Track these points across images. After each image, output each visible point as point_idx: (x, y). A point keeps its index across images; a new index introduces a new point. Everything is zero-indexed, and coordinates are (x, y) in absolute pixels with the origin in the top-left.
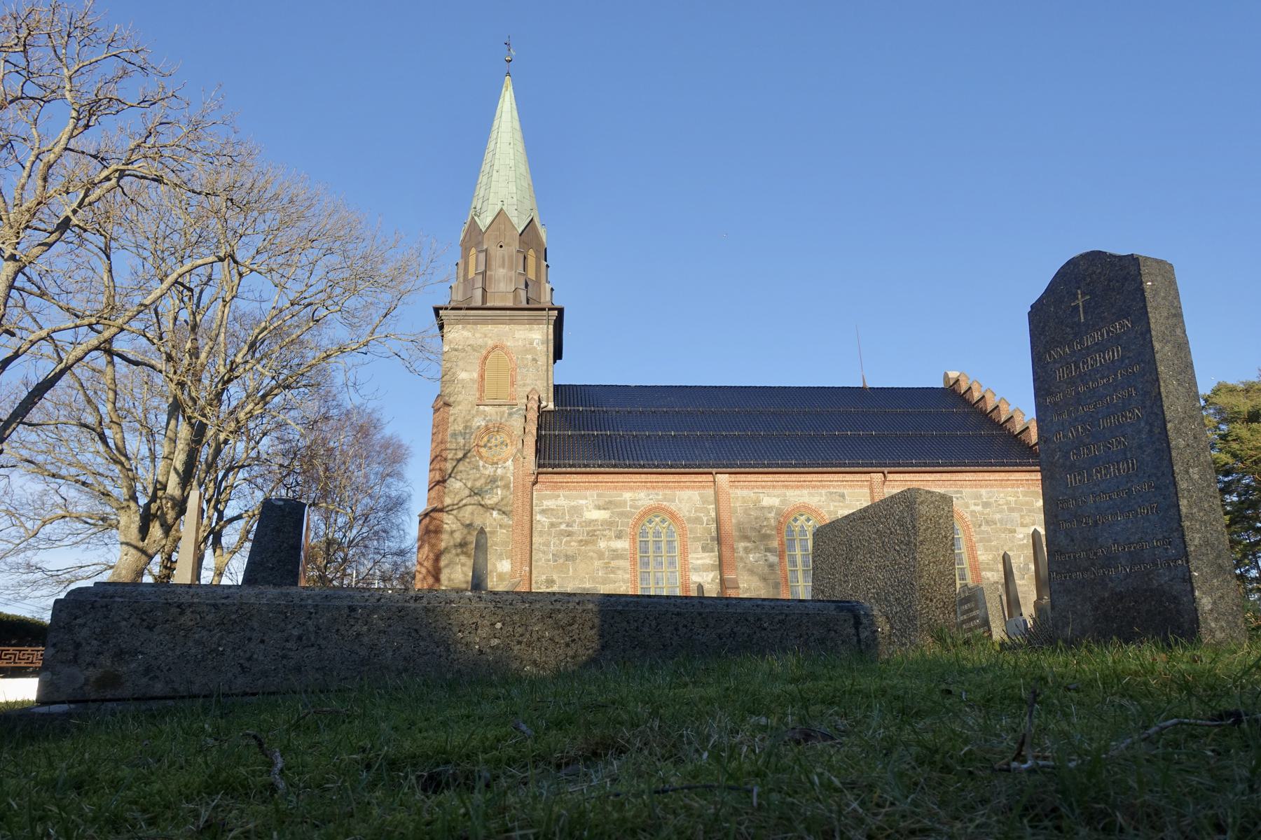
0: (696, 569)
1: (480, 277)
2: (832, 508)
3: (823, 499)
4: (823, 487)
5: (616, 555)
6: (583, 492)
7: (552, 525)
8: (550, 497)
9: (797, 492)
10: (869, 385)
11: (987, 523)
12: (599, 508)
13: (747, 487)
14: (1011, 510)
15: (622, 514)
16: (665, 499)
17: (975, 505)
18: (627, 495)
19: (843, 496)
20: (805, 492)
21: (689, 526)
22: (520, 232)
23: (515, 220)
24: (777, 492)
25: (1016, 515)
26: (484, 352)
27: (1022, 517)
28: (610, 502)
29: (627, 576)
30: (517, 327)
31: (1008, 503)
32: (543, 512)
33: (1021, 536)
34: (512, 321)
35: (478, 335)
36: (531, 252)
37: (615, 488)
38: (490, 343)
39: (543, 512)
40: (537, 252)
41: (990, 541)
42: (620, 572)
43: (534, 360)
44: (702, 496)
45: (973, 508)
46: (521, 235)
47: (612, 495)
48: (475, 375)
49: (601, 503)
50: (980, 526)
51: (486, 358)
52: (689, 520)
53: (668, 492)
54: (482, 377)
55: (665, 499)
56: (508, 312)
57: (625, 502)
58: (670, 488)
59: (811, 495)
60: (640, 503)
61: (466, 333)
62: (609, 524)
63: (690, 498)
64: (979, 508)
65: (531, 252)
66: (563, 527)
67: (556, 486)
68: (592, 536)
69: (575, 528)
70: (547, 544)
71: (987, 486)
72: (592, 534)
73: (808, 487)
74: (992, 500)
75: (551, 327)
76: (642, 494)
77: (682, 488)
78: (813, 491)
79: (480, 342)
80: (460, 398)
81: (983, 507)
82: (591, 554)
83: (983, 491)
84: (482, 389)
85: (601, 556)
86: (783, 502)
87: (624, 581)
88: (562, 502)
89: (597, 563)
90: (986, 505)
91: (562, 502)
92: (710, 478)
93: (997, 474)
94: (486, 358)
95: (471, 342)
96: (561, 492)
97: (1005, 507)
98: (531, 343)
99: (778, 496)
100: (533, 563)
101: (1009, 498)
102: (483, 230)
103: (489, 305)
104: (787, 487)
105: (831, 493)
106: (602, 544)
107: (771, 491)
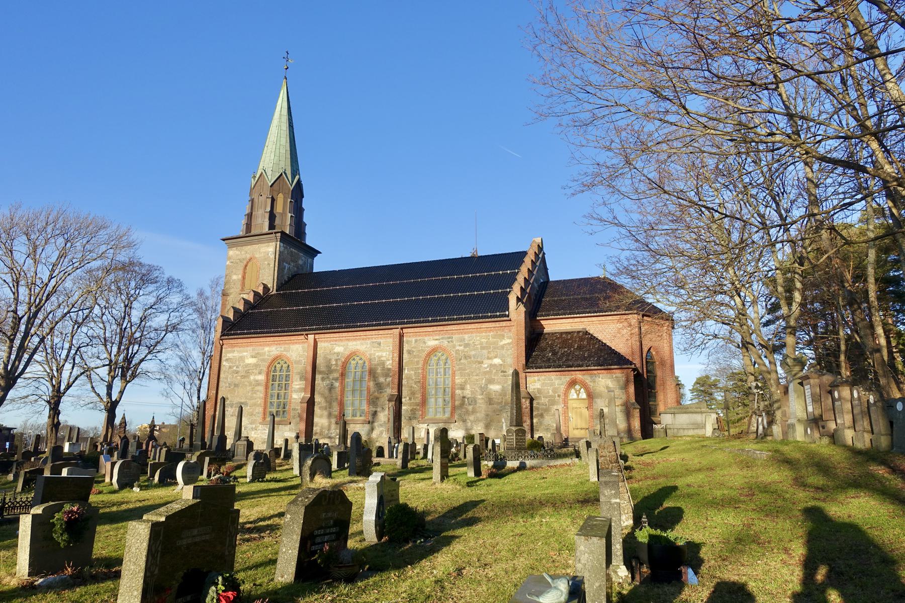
2: (373, 352)
3: (368, 346)
4: (369, 338)
5: (258, 383)
6: (246, 348)
7: (230, 367)
8: (230, 352)
9: (354, 343)
11: (465, 358)
12: (252, 357)
13: (327, 341)
14: (483, 348)
15: (263, 360)
16: (285, 350)
17: (460, 346)
18: (267, 349)
19: (379, 344)
20: (358, 342)
21: (294, 365)
22: (270, 184)
24: (342, 343)
25: (485, 352)
26: (245, 262)
27: (489, 352)
28: (258, 353)
30: (262, 245)
31: (481, 343)
32: (227, 360)
33: (486, 366)
34: (260, 242)
35: (243, 253)
36: (281, 196)
37: (261, 345)
38: (248, 256)
39: (227, 360)
40: (284, 194)
41: (465, 370)
42: (258, 393)
43: (269, 264)
44: (303, 348)
45: (458, 348)
46: (271, 186)
47: (259, 349)
48: (240, 276)
49: (253, 354)
50: (461, 359)
51: (246, 266)
53: (286, 346)
54: (244, 278)
55: (285, 350)
56: (257, 237)
57: (265, 353)
58: (287, 344)
59: (362, 344)
60: (272, 353)
61: (238, 252)
63: (297, 349)
64: (461, 348)
65: (281, 196)
66: (235, 368)
67: (233, 346)
68: (247, 374)
69: (240, 369)
70: (226, 378)
71: (468, 333)
72: (247, 372)
73: (359, 339)
74: (471, 342)
75: (278, 243)
76: (273, 348)
77: (293, 343)
78: (363, 342)
79: (244, 256)
80: (232, 291)
81: (465, 347)
82: (246, 383)
83: (466, 336)
84: (243, 284)
85: (250, 384)
86: (345, 349)
87: (260, 398)
88: (236, 354)
89: (249, 388)
90: (467, 345)
91: (236, 354)
92: (302, 337)
93: (473, 325)
94: (246, 266)
96: (236, 349)
97: (479, 346)
99: (343, 346)
100: (220, 389)
101: (483, 340)
103: (253, 233)
104: (348, 340)
105: (373, 342)
107: (340, 343)
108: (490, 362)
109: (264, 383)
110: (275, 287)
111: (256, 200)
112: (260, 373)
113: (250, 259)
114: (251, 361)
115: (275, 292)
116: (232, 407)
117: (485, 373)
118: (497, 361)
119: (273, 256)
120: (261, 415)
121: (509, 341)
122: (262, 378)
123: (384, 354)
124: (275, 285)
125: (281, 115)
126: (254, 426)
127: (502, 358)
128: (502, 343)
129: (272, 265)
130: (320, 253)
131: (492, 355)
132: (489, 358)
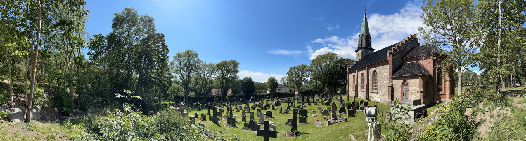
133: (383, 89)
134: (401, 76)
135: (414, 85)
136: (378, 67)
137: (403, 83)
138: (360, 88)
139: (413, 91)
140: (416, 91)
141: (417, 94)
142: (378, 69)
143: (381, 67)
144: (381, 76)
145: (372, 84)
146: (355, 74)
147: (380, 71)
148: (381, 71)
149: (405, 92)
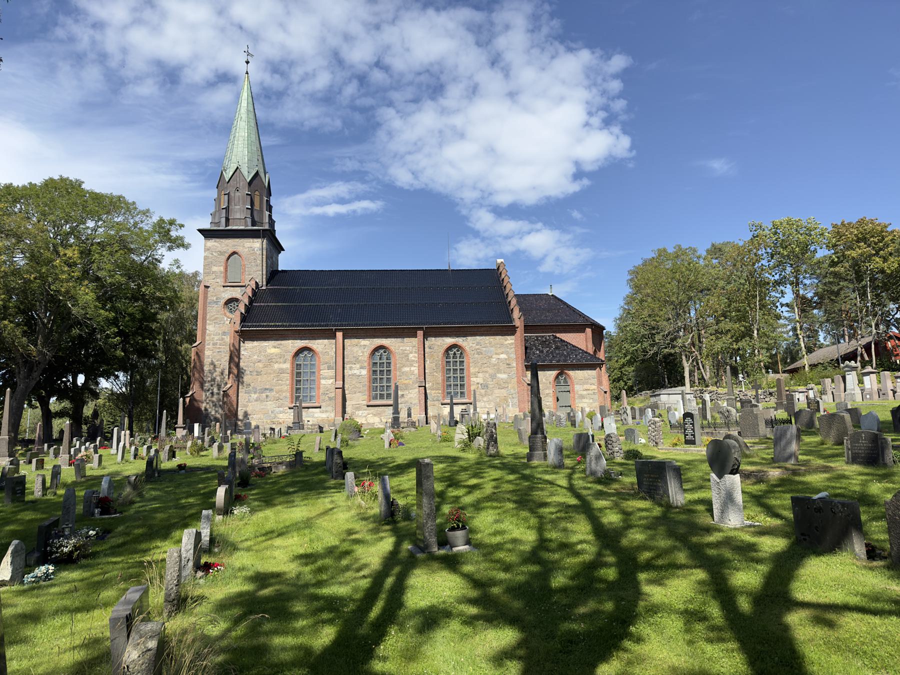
0: (325, 378)
1: (224, 210)
5: (282, 371)
10: (452, 268)
22: (248, 180)
23: (245, 173)
25: (493, 349)
26: (227, 255)
29: (288, 382)
38: (231, 251)
46: (250, 183)
52: (322, 352)
61: (216, 244)
62: (281, 356)
66: (256, 357)
69: (262, 358)
79: (225, 249)
84: (226, 277)
94: (228, 259)
95: (219, 249)
98: (253, 250)
102: (227, 180)
106: (276, 366)
108: (498, 356)
109: (289, 371)
110: (265, 283)
111: (232, 194)
112: (285, 362)
113: (234, 253)
114: (273, 351)
115: (264, 288)
116: (255, 393)
117: (495, 365)
118: (503, 356)
119: (260, 252)
120: (289, 400)
121: (513, 341)
122: (287, 366)
123: (408, 348)
124: (264, 280)
125: (248, 111)
126: (281, 409)
127: (507, 353)
128: (506, 343)
129: (259, 262)
130: (283, 250)
131: (499, 351)
132: (496, 354)
133: (497, 391)
134: (554, 362)
135: (585, 381)
136: (469, 338)
137: (557, 377)
138: (366, 397)
139: (585, 392)
140: (590, 392)
141: (593, 396)
142: (468, 343)
143: (482, 337)
144: (485, 362)
145: (443, 380)
146: (318, 345)
147: (477, 347)
148: (484, 349)
149: (560, 396)
